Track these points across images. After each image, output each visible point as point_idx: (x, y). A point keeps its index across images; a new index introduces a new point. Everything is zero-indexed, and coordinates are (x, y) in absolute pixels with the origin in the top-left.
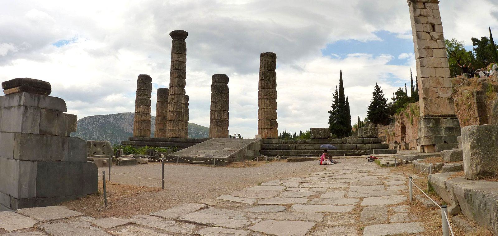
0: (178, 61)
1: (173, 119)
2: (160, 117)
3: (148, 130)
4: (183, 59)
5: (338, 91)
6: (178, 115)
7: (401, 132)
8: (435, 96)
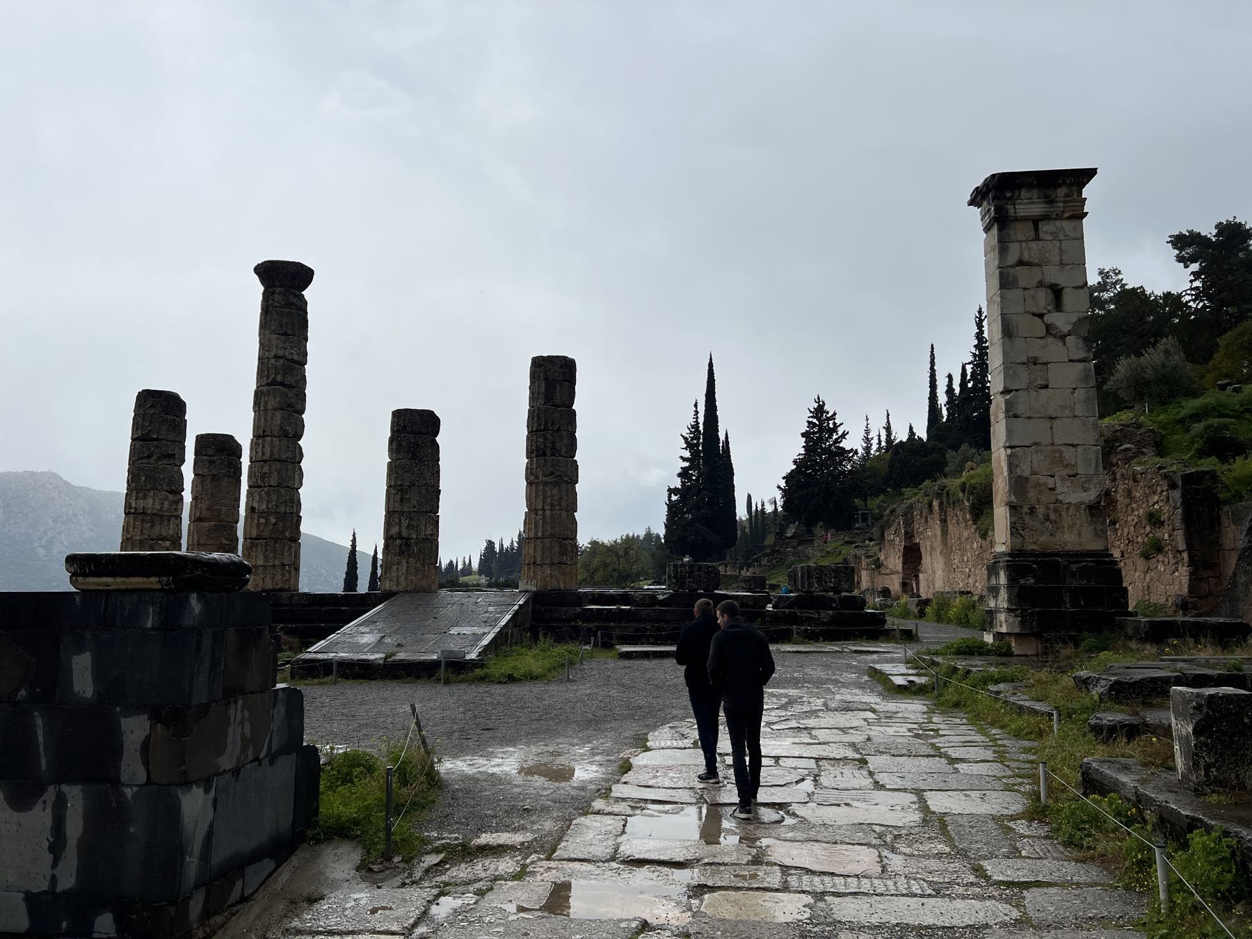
0: (284, 357)
1: (266, 533)
2: (206, 524)
5: (701, 428)
6: (281, 524)
7: (904, 563)
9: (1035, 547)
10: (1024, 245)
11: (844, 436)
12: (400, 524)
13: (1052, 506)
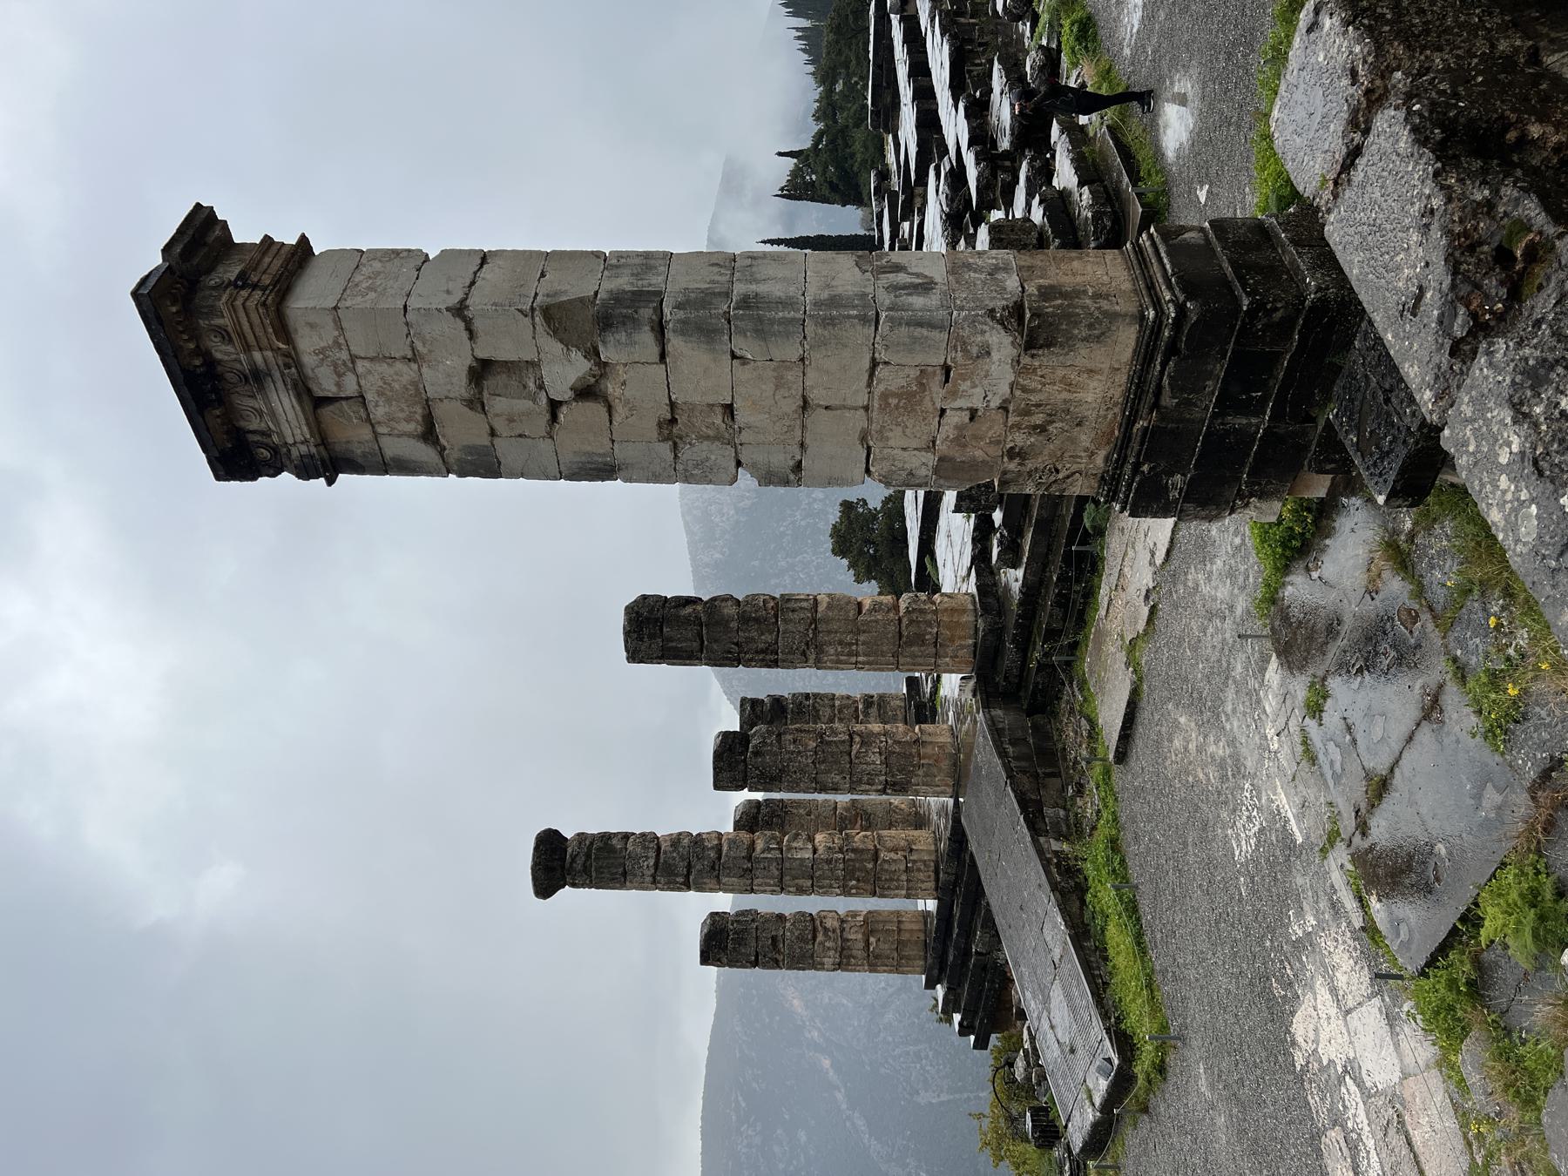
3: (900, 930)
4: (647, 858)
8: (993, 427)
9: (1102, 453)
10: (380, 430)
13: (1012, 419)
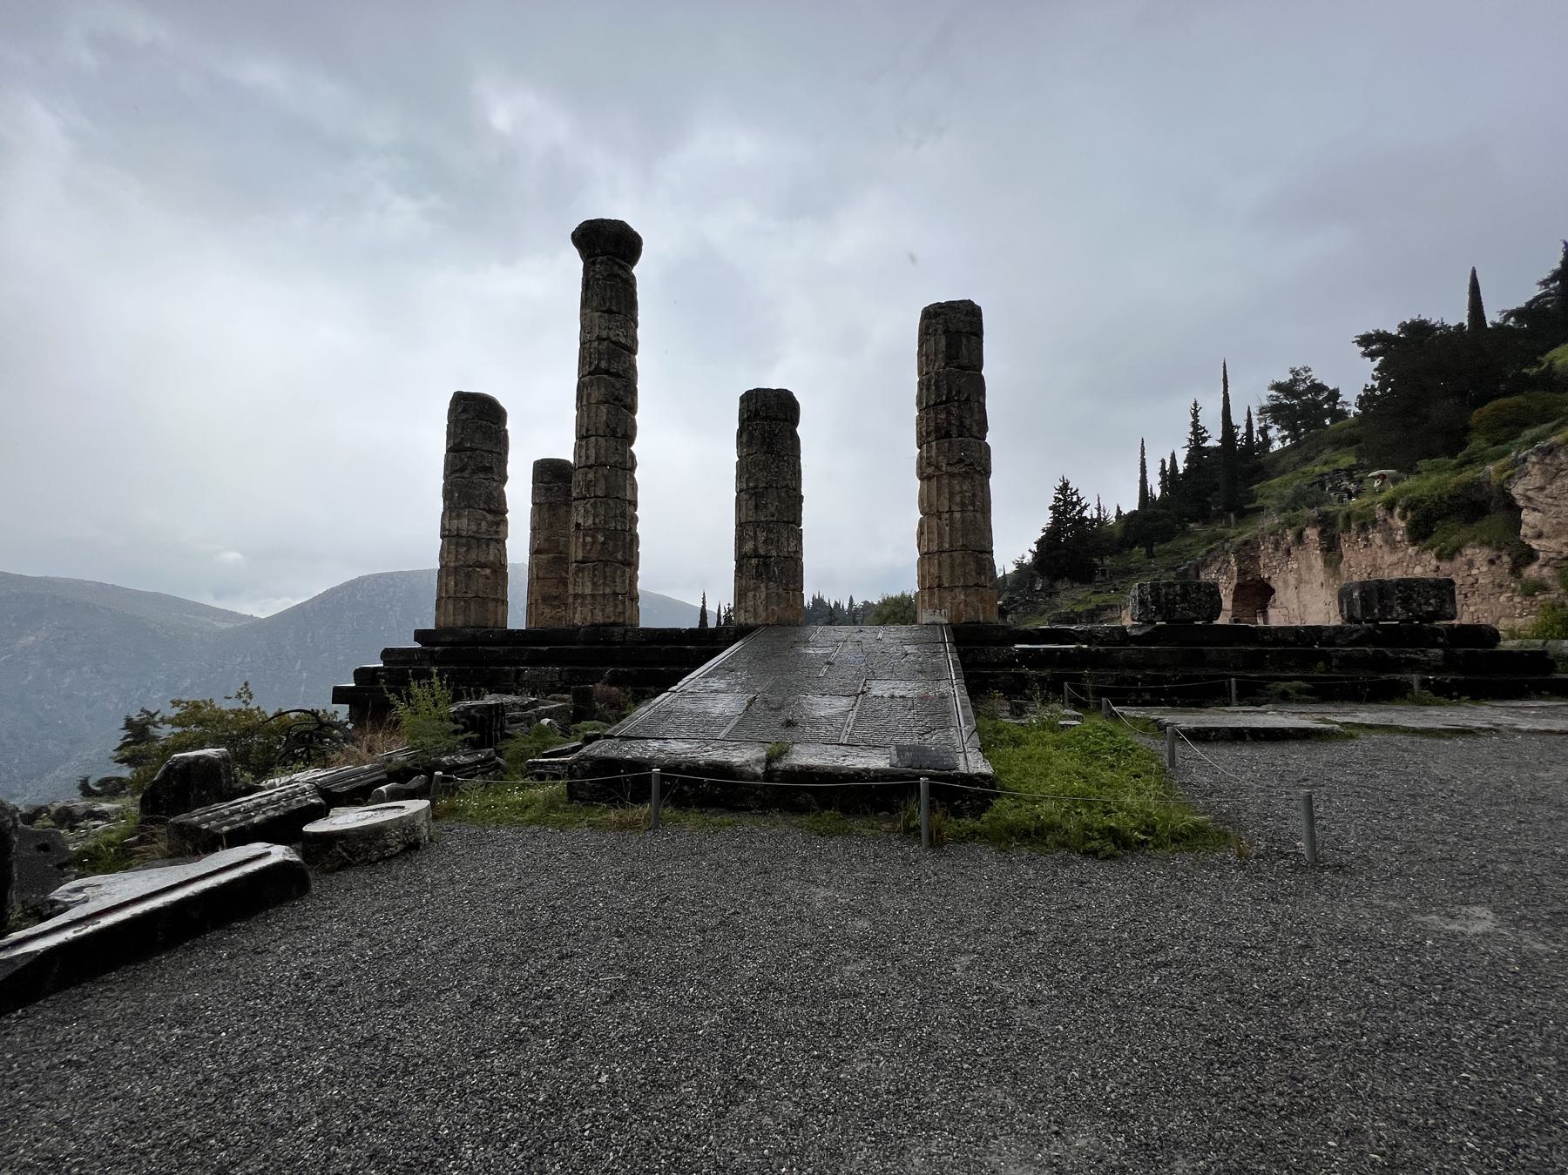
1: (593, 555)
3: (497, 600)
7: (1234, 600)
11: (1085, 507)
12: (755, 539)
